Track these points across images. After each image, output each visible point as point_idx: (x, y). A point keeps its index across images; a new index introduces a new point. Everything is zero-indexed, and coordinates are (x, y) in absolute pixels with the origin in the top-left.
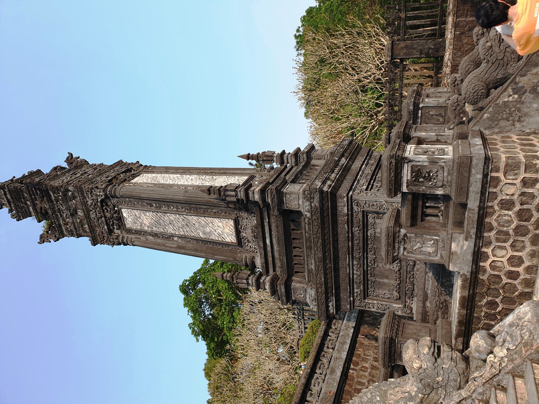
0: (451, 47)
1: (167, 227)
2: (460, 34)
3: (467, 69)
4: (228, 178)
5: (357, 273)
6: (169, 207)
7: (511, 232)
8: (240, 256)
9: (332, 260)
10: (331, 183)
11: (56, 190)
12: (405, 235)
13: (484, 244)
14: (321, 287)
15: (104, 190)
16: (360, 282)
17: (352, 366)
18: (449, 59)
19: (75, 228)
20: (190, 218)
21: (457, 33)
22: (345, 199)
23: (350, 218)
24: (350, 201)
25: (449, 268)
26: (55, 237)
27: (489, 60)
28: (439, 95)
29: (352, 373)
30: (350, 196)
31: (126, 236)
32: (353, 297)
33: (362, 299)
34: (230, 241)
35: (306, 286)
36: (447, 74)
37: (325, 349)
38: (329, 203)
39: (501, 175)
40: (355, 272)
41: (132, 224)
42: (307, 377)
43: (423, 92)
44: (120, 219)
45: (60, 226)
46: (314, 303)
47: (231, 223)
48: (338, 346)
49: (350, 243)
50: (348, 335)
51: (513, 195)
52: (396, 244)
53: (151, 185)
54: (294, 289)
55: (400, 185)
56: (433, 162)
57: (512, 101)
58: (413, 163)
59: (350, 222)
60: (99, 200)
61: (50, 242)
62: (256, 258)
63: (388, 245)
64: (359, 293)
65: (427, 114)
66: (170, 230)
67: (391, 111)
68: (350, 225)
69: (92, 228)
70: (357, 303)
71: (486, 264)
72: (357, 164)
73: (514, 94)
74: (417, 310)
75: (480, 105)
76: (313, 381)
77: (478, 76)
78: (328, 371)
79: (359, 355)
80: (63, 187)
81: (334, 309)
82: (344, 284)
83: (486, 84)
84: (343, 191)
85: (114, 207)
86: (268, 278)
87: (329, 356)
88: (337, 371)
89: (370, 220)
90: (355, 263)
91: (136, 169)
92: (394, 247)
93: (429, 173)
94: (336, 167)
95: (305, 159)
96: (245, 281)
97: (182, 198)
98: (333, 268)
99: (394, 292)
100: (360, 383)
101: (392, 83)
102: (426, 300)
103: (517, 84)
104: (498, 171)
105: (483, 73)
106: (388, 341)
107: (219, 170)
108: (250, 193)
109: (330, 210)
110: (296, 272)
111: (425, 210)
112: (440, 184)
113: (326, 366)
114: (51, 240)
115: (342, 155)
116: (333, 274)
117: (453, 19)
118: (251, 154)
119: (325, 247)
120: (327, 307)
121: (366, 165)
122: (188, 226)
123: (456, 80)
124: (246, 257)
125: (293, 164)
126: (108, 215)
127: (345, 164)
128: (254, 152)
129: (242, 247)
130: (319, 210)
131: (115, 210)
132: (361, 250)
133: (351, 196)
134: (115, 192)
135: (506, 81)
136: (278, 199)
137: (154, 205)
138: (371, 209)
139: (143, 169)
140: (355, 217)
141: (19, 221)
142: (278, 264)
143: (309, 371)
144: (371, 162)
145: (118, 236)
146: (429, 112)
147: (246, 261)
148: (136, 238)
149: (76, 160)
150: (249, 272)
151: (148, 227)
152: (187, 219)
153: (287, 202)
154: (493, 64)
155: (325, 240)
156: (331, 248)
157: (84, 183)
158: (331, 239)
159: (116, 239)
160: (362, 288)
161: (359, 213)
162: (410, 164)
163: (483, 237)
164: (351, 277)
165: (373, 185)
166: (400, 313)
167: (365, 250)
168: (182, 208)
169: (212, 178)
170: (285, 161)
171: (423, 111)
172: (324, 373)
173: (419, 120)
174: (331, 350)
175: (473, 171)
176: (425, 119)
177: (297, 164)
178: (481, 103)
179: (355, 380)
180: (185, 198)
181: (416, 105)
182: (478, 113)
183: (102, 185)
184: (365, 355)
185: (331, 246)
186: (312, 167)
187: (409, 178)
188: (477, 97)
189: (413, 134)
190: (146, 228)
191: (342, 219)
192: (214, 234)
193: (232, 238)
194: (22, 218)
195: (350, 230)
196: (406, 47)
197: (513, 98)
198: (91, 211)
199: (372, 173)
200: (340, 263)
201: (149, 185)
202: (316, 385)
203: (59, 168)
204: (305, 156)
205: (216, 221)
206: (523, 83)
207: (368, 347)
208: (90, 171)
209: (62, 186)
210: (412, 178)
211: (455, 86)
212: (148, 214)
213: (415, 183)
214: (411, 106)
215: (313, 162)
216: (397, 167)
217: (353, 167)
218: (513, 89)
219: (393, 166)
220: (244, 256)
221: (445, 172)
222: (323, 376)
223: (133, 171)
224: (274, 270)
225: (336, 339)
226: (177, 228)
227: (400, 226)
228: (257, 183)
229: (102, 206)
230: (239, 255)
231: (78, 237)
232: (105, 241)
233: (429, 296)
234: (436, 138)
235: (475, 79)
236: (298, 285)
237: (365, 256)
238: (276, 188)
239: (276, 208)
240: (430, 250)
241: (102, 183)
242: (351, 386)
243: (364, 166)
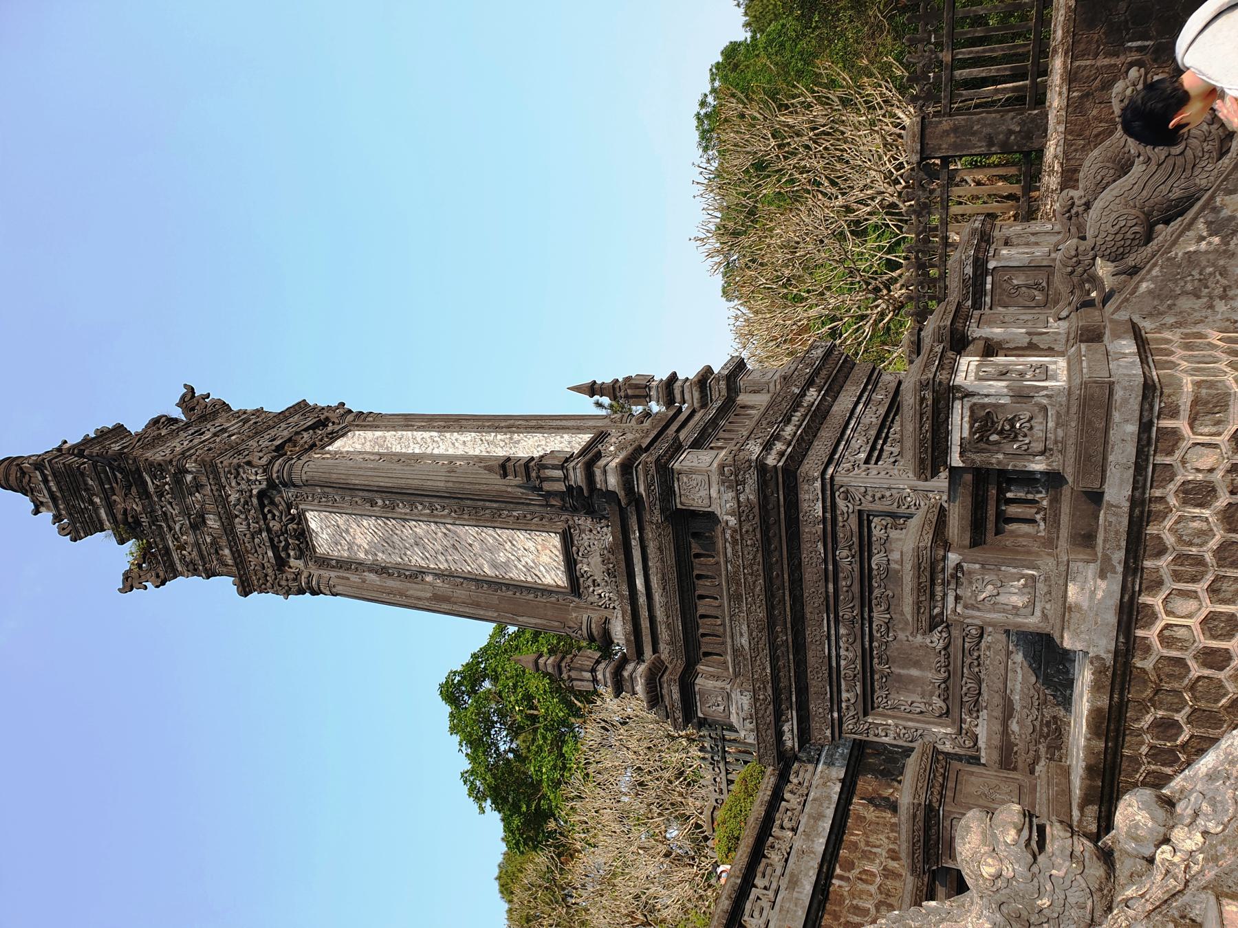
0: (1061, 128)
1: (408, 553)
2: (1081, 97)
3: (1099, 178)
4: (546, 438)
5: (848, 656)
6: (412, 505)
7: (1209, 557)
8: (576, 617)
9: (789, 625)
10: (784, 447)
11: (158, 469)
12: (958, 567)
13: (1144, 586)
14: (765, 687)
15: (266, 469)
16: (855, 676)
17: (838, 871)
18: (1056, 157)
19: (202, 557)
20: (460, 530)
21: (1075, 94)
22: (818, 484)
23: (829, 528)
24: (830, 489)
25: (1062, 642)
26: (158, 576)
27: (1151, 156)
28: (1033, 239)
29: (839, 886)
30: (828, 476)
31: (316, 573)
32: (839, 711)
33: (861, 715)
34: (552, 582)
35: (728, 687)
36: (1053, 191)
37: (776, 831)
38: (781, 493)
39: (1182, 424)
40: (843, 652)
41: (329, 546)
42: (733, 896)
43: (996, 233)
44: (303, 535)
45: (167, 551)
47: (556, 540)
48: (807, 824)
49: (831, 586)
50: (829, 797)
51: (1211, 470)
52: (938, 589)
53: (372, 458)
54: (702, 693)
55: (946, 451)
56: (1022, 396)
57: (1206, 252)
58: (975, 400)
59: (830, 538)
60: (255, 492)
61: (146, 588)
62: (613, 621)
63: (919, 589)
64: (852, 701)
65: (1005, 285)
66: (416, 559)
67: (921, 278)
68: (830, 545)
69: (240, 556)
70: (848, 725)
71: (1152, 634)
72: (844, 402)
73: (1211, 235)
74: (989, 739)
75: (1131, 261)
76: (748, 906)
77: (1126, 195)
78: (784, 883)
79: (855, 844)
80: (174, 464)
81: (796, 739)
82: (817, 682)
83: (1143, 212)
84: (811, 466)
85: (289, 506)
86: (642, 668)
87: (785, 847)
88: (805, 883)
89: (877, 532)
90: (842, 631)
91: (337, 421)
92: (933, 595)
93: (1012, 422)
94: (796, 411)
95: (724, 392)
96: (588, 675)
97: (442, 484)
98: (791, 644)
99: (935, 699)
100: (857, 910)
101: (924, 213)
102: (1010, 716)
103: (1219, 212)
104: (1174, 413)
105: (1136, 186)
106: (921, 814)
107: (527, 420)
108: (598, 472)
109: (782, 509)
110: (706, 654)
111: (1004, 508)
112: (1038, 446)
113: (779, 871)
115: (810, 383)
116: (791, 657)
117: (1065, 63)
118: (599, 382)
119: (773, 596)
120: (779, 734)
121: (866, 405)
122: (457, 549)
123: (1073, 204)
124: (590, 620)
125: (696, 405)
126: (275, 525)
127: (816, 403)
128: (605, 378)
129: (580, 596)
130: (756, 510)
131: (290, 514)
132: (857, 602)
133: (832, 477)
134: (290, 474)
135: (1192, 206)
136: (660, 485)
137: (380, 502)
138: (877, 506)
139: (354, 420)
140: (841, 524)
141: (75, 541)
142: (664, 635)
143: (739, 881)
144: (878, 397)
145: (299, 574)
146: (1010, 279)
147: (589, 628)
148: (338, 577)
149: (201, 401)
150: (597, 655)
151: (366, 553)
152: (455, 533)
153: (682, 492)
154: (1159, 165)
155: (771, 579)
156: (787, 598)
157: (221, 453)
158: (786, 576)
159: (295, 580)
160: (859, 689)
161: (851, 516)
162: (968, 403)
163: (1142, 569)
164: (834, 664)
165: (882, 450)
166: (948, 747)
167: (865, 600)
168: (444, 508)
169: (511, 438)
170: (678, 397)
171: (997, 278)
172: (774, 886)
173: (988, 299)
174: (790, 834)
175: (1116, 417)
176: (1000, 295)
177: (704, 405)
178: (1133, 256)
179: (847, 902)
180: (450, 485)
181: (980, 265)
182: (1125, 281)
183: (260, 458)
184: (867, 843)
185: (787, 593)
186: (739, 411)
187: (966, 434)
188: (1122, 242)
189: (974, 331)
190: (362, 555)
191: (811, 531)
192: (516, 566)
193: (557, 575)
194: (82, 535)
195: (830, 556)
196: (955, 129)
197: (1210, 243)
198: (237, 516)
199: (879, 422)
200: (807, 633)
201: (367, 457)
202: (756, 914)
203: (163, 419)
204: (723, 384)
205: (521, 537)
206: (1231, 208)
207: (876, 826)
208: (233, 425)
209: (171, 461)
210: (972, 433)
211: (1070, 218)
212: (365, 523)
213: (978, 445)
214: (968, 267)
215: (743, 398)
216: (938, 408)
217: (834, 408)
218: (1209, 224)
219: (927, 406)
221: (1050, 419)
222: (771, 894)
223: (330, 424)
224: (655, 650)
225: (800, 807)
226: (433, 553)
227: (947, 546)
228: (612, 448)
229: (262, 506)
230: (574, 615)
231: (208, 578)
232: (268, 584)
233: (1017, 707)
234: (1028, 340)
235: (1117, 201)
236: (710, 684)
237: (866, 616)
238: (657, 460)
239: (658, 507)
240: (1018, 600)
241: (261, 454)
242: (836, 917)
243: (861, 406)
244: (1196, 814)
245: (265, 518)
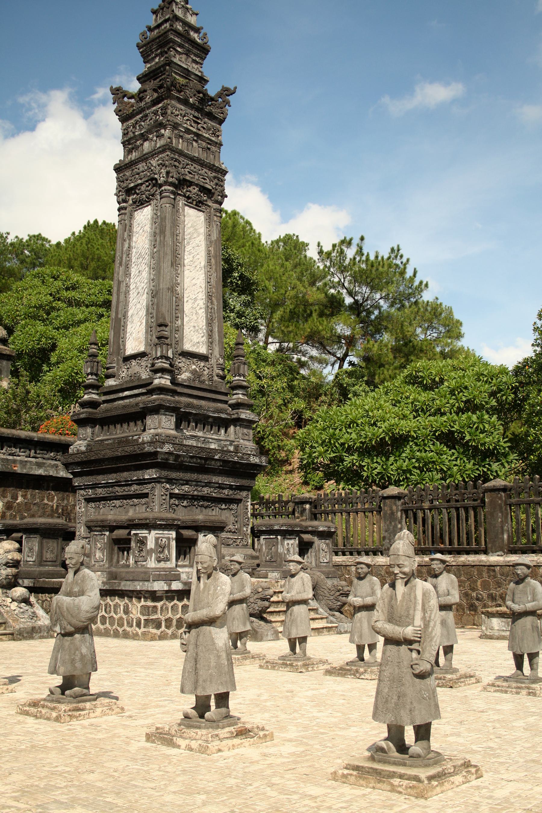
7: (111, 615)
22: (155, 476)
44: (140, 204)
46: (75, 449)
47: (142, 349)
59: (141, 482)
61: (114, 103)
78: (40, 460)
93: (142, 550)
114: (116, 105)
137: (155, 250)
141: (137, 46)
170: (235, 392)
191: (135, 475)
194: (141, 50)
220: (114, 365)
224: (105, 402)
228: (194, 367)
240: (97, 556)
244: (21, 608)
245: (147, 181)
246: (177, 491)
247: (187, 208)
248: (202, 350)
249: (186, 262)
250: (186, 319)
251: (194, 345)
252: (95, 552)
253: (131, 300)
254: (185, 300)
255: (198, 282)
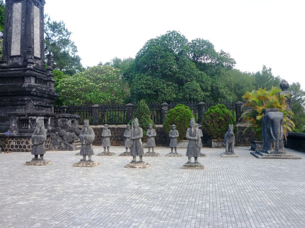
20: (20, 35)
22: (29, 99)
47: (19, 54)
71: (10, 140)
142: (5, 73)
227: (19, 117)
228: (37, 62)
246: (35, 104)
247: (34, 6)
248: (39, 56)
249: (35, 25)
250: (35, 45)
251: (37, 55)
252: (12, 124)
253: (13, 36)
254: (34, 39)
255: (38, 33)
